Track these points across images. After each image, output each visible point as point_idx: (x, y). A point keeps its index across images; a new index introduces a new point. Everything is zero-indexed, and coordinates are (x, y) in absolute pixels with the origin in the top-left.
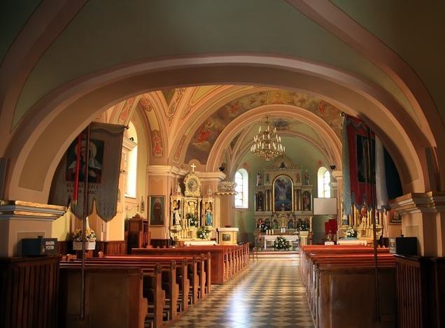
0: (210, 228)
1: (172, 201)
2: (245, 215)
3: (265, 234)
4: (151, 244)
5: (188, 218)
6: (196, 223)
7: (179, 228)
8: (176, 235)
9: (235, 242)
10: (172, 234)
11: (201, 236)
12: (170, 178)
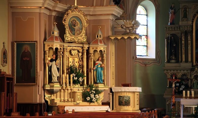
0: (101, 87)
1: (47, 49)
2: (150, 69)
3: (182, 97)
4: (18, 111)
5: (69, 73)
6: (81, 79)
7: (57, 86)
8: (53, 97)
9: (137, 107)
10: (47, 96)
11: (88, 99)
12: (42, 16)
